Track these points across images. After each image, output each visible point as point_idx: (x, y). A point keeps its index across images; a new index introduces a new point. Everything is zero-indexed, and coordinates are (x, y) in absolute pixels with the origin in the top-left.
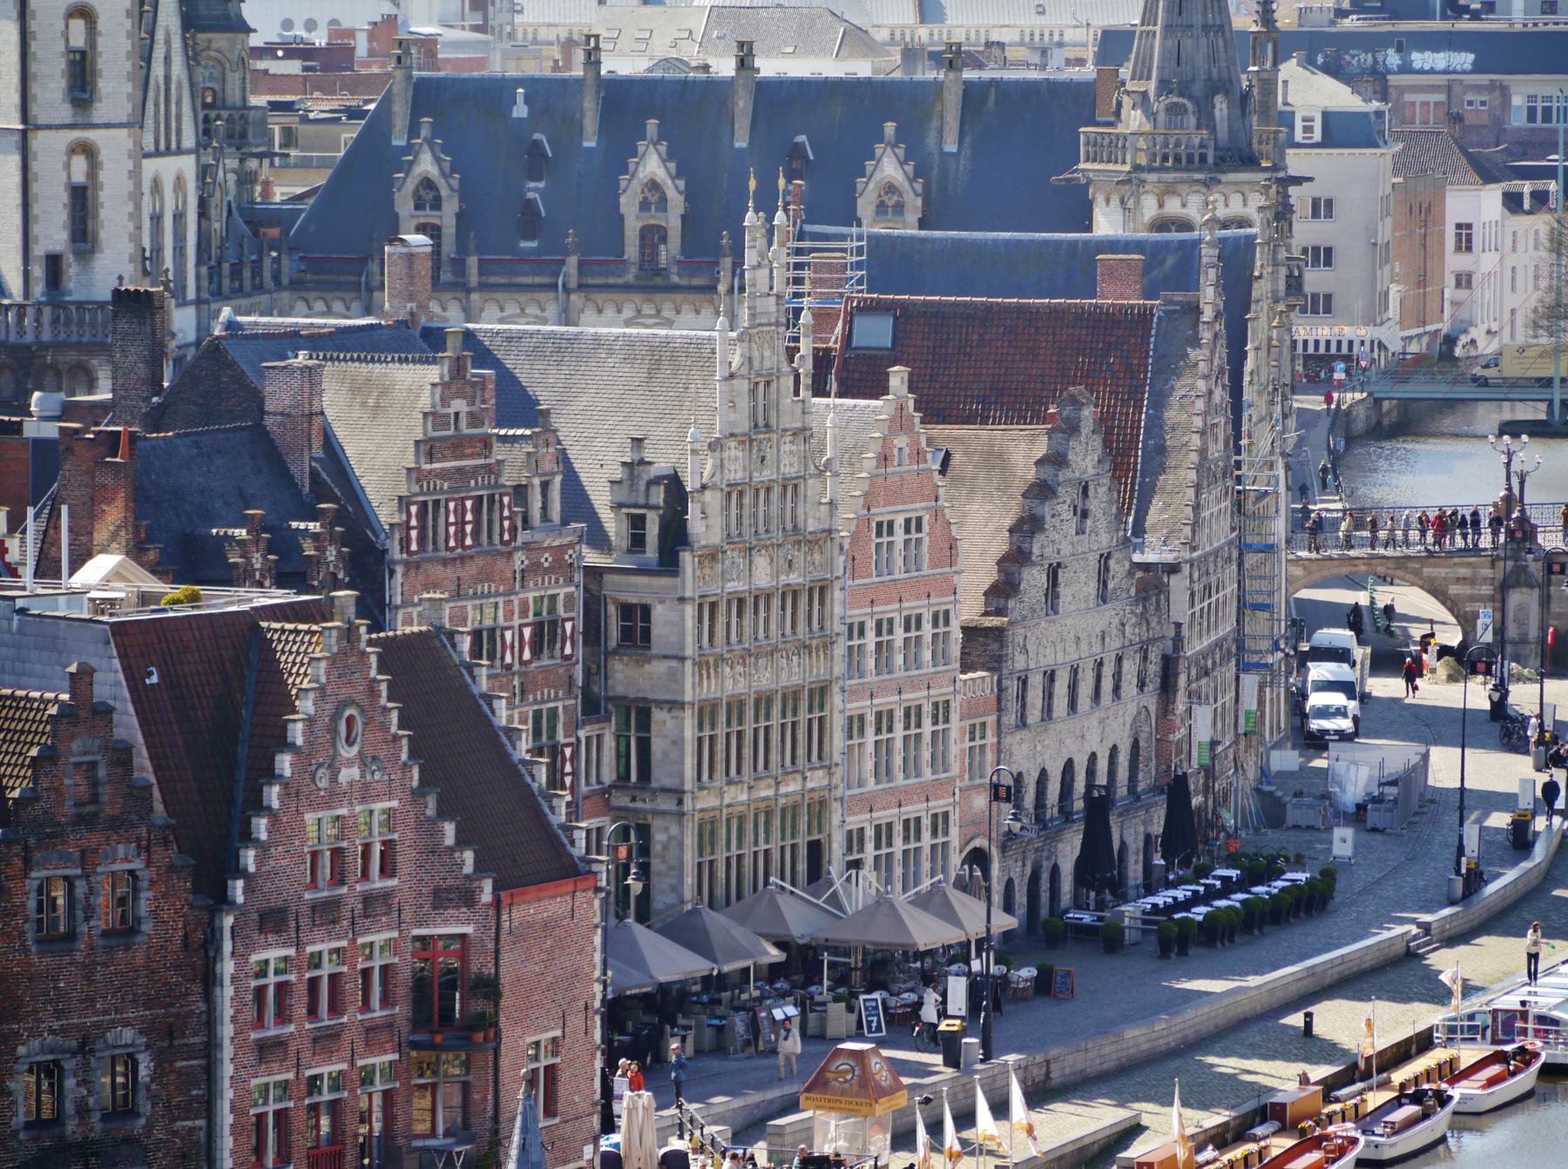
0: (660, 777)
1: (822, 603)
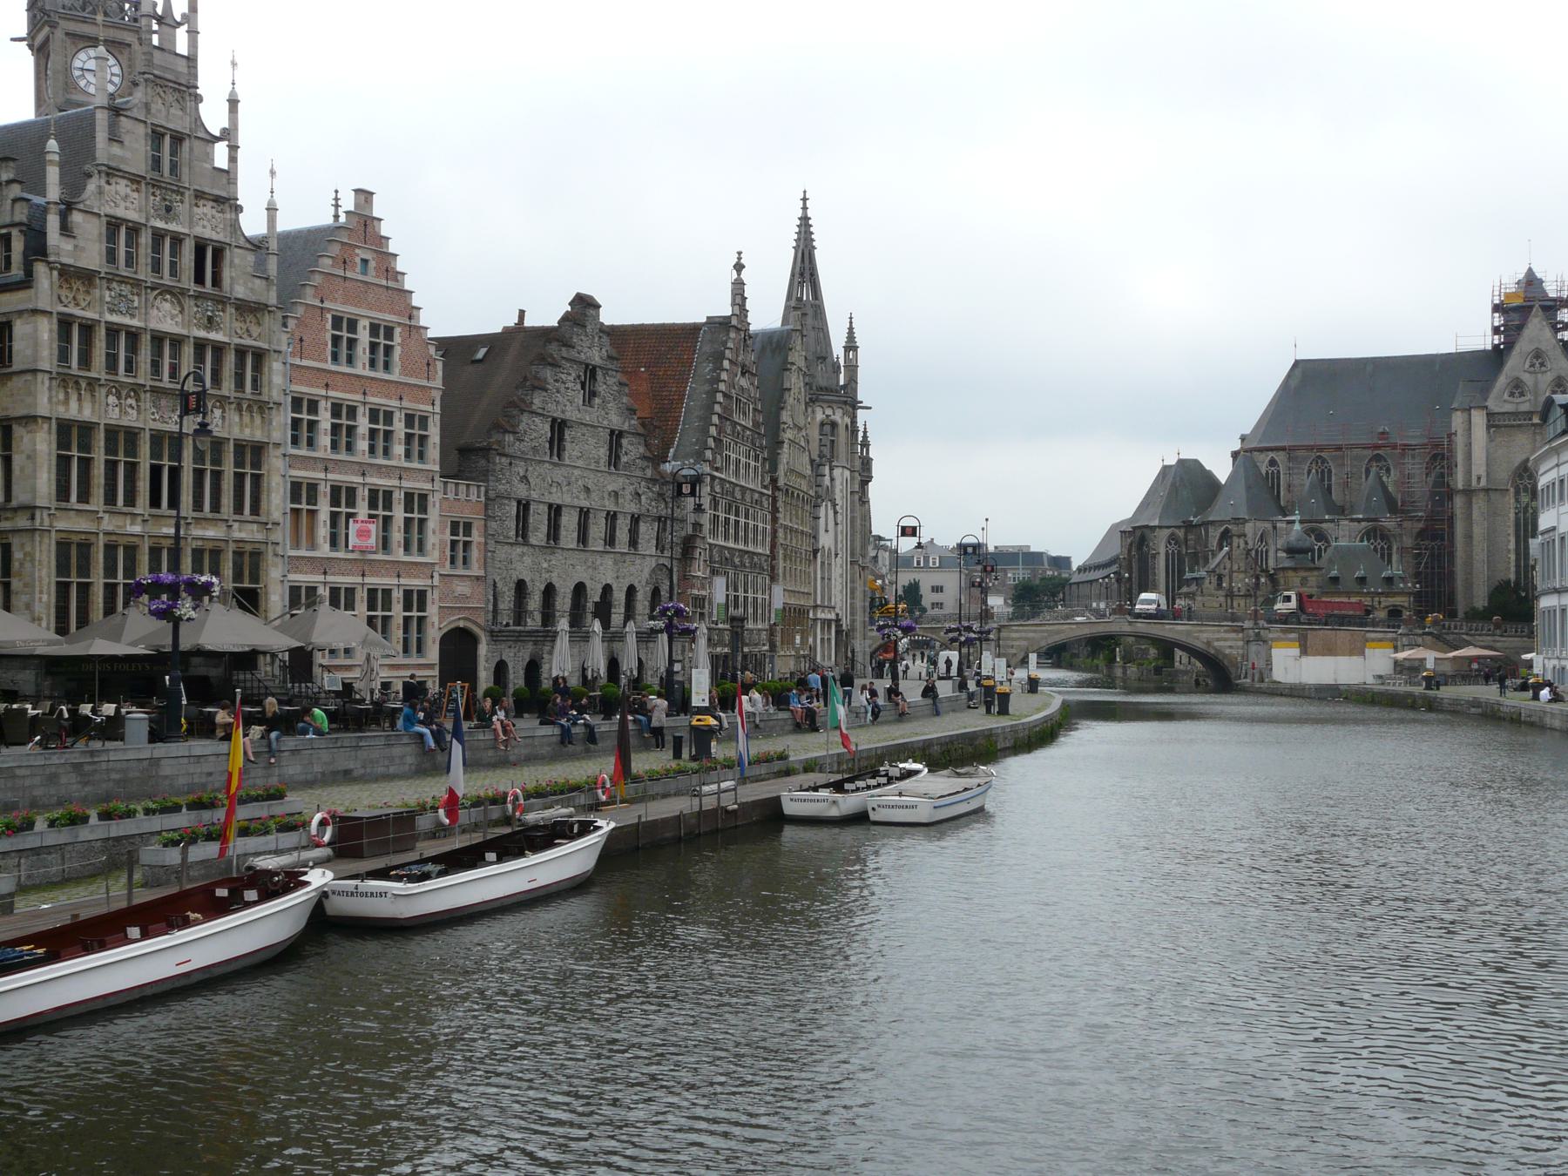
0: (20, 497)
1: (257, 368)
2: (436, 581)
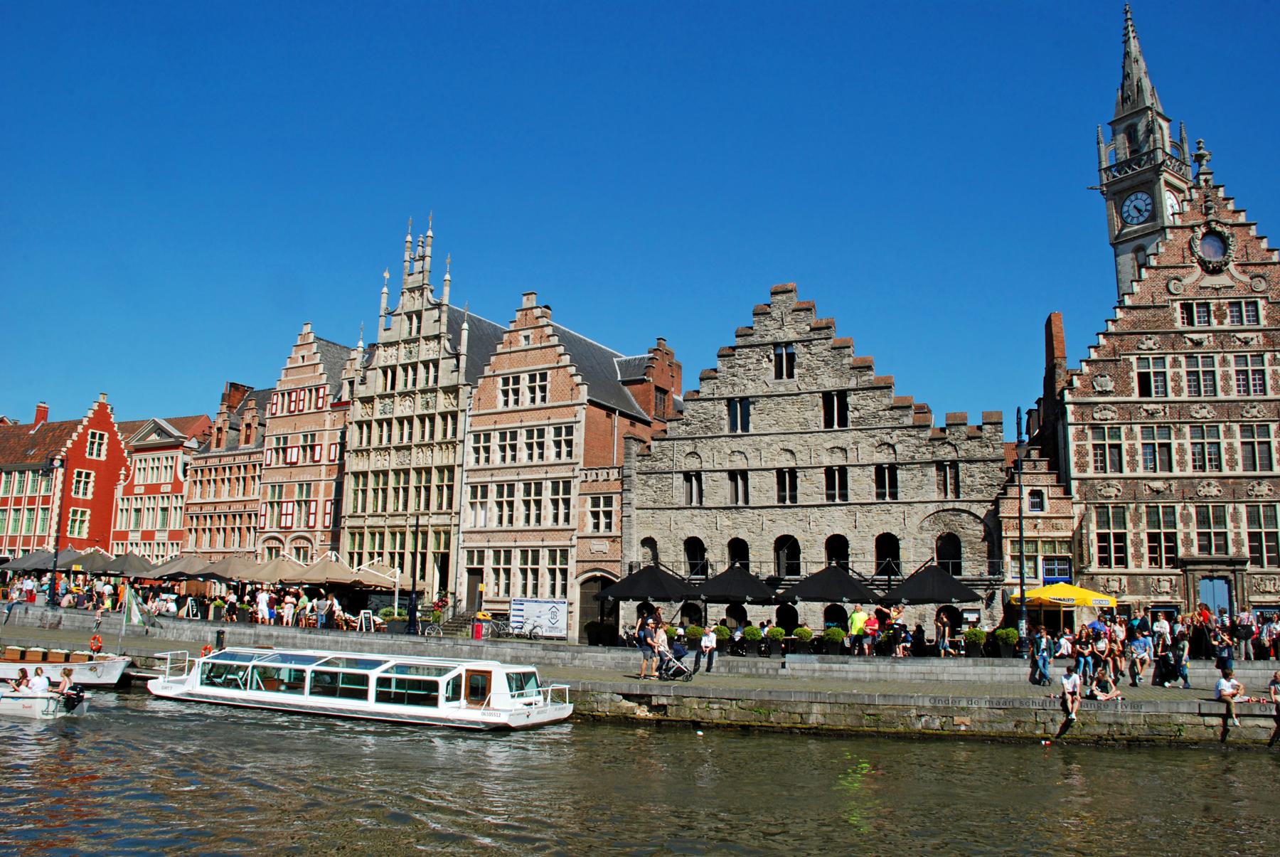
2: (575, 541)
